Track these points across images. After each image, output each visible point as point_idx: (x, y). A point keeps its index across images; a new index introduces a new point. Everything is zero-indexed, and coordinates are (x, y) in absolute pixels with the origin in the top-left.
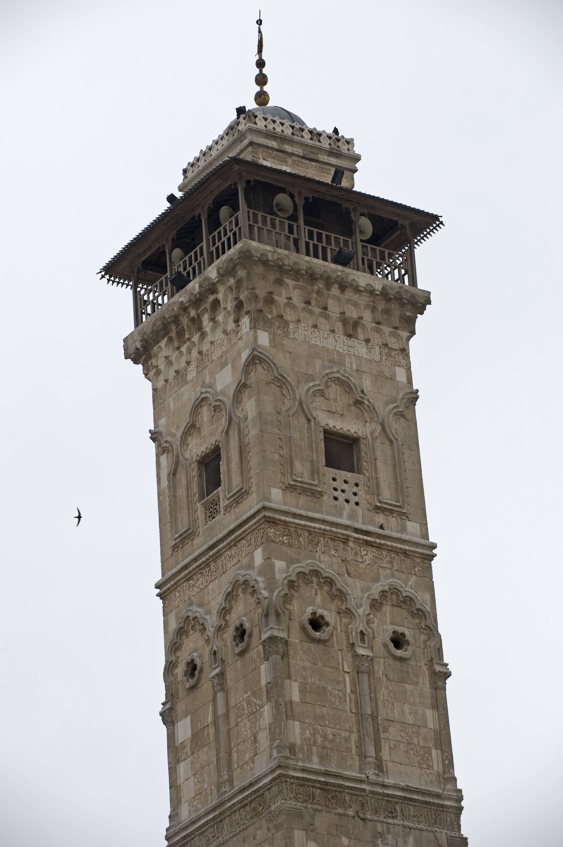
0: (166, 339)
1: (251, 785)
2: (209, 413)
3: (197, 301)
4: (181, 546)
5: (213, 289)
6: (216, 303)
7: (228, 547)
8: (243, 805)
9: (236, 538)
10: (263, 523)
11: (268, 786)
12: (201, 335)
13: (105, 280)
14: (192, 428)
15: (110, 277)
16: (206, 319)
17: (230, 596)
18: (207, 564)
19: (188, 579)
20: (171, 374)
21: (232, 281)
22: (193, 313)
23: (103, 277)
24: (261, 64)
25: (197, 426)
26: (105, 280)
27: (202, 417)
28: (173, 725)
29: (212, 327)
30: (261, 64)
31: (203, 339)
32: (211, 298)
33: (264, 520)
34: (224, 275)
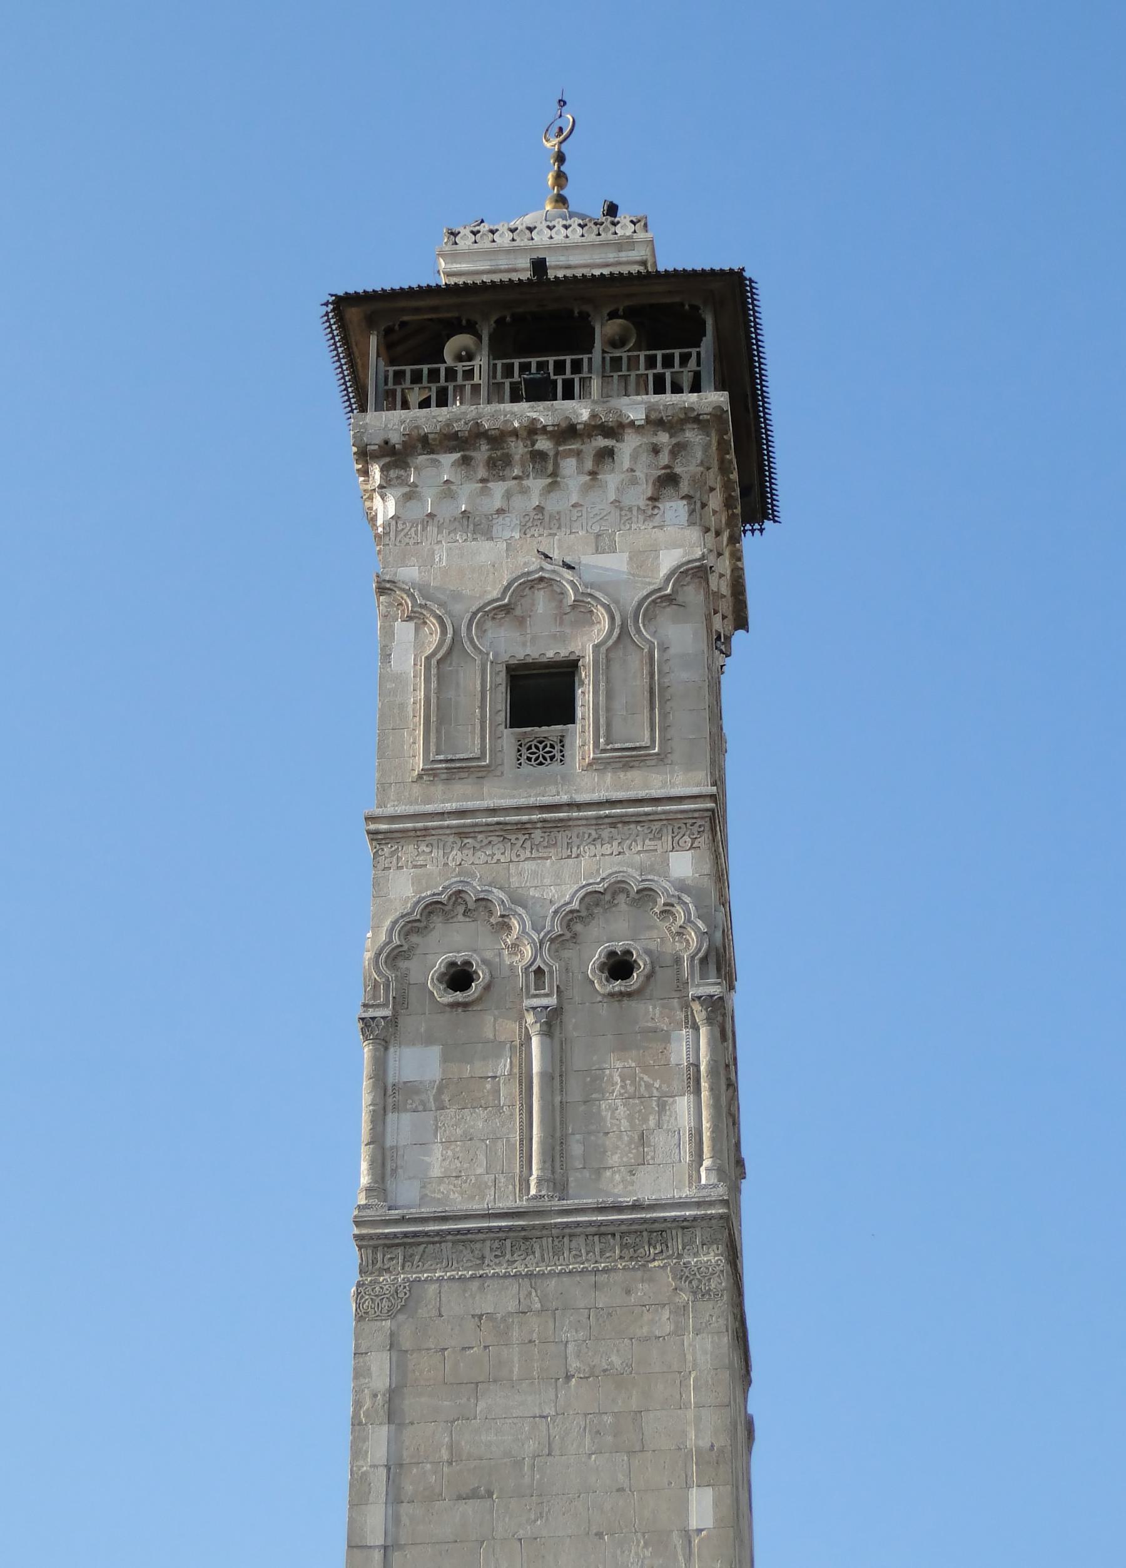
0: (459, 455)
1: (636, 1207)
2: (554, 604)
3: (569, 432)
4: (444, 776)
5: (614, 430)
6: (607, 454)
7: (594, 822)
8: (602, 1232)
9: (622, 816)
10: (702, 818)
11: (685, 1224)
12: (550, 484)
13: (324, 309)
14: (504, 610)
15: (333, 310)
16: (569, 466)
17: (597, 902)
18: (523, 828)
19: (461, 834)
20: (447, 511)
21: (663, 438)
22: (543, 444)
23: (326, 304)
24: (561, 158)
25: (518, 612)
26: (324, 309)
27: (533, 605)
28: (386, 1049)
29: (585, 483)
30: (561, 158)
31: (549, 492)
32: (601, 442)
33: (709, 814)
34: (656, 423)
